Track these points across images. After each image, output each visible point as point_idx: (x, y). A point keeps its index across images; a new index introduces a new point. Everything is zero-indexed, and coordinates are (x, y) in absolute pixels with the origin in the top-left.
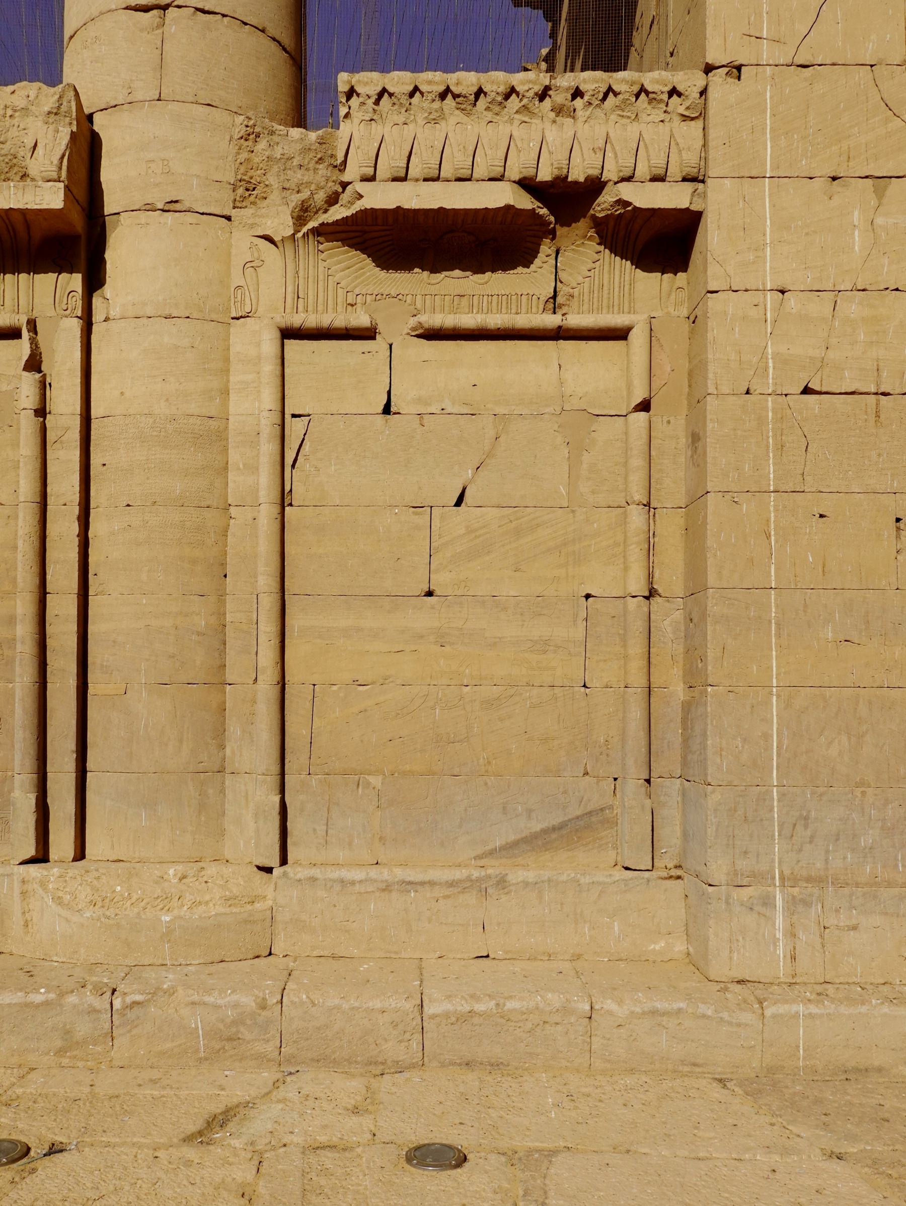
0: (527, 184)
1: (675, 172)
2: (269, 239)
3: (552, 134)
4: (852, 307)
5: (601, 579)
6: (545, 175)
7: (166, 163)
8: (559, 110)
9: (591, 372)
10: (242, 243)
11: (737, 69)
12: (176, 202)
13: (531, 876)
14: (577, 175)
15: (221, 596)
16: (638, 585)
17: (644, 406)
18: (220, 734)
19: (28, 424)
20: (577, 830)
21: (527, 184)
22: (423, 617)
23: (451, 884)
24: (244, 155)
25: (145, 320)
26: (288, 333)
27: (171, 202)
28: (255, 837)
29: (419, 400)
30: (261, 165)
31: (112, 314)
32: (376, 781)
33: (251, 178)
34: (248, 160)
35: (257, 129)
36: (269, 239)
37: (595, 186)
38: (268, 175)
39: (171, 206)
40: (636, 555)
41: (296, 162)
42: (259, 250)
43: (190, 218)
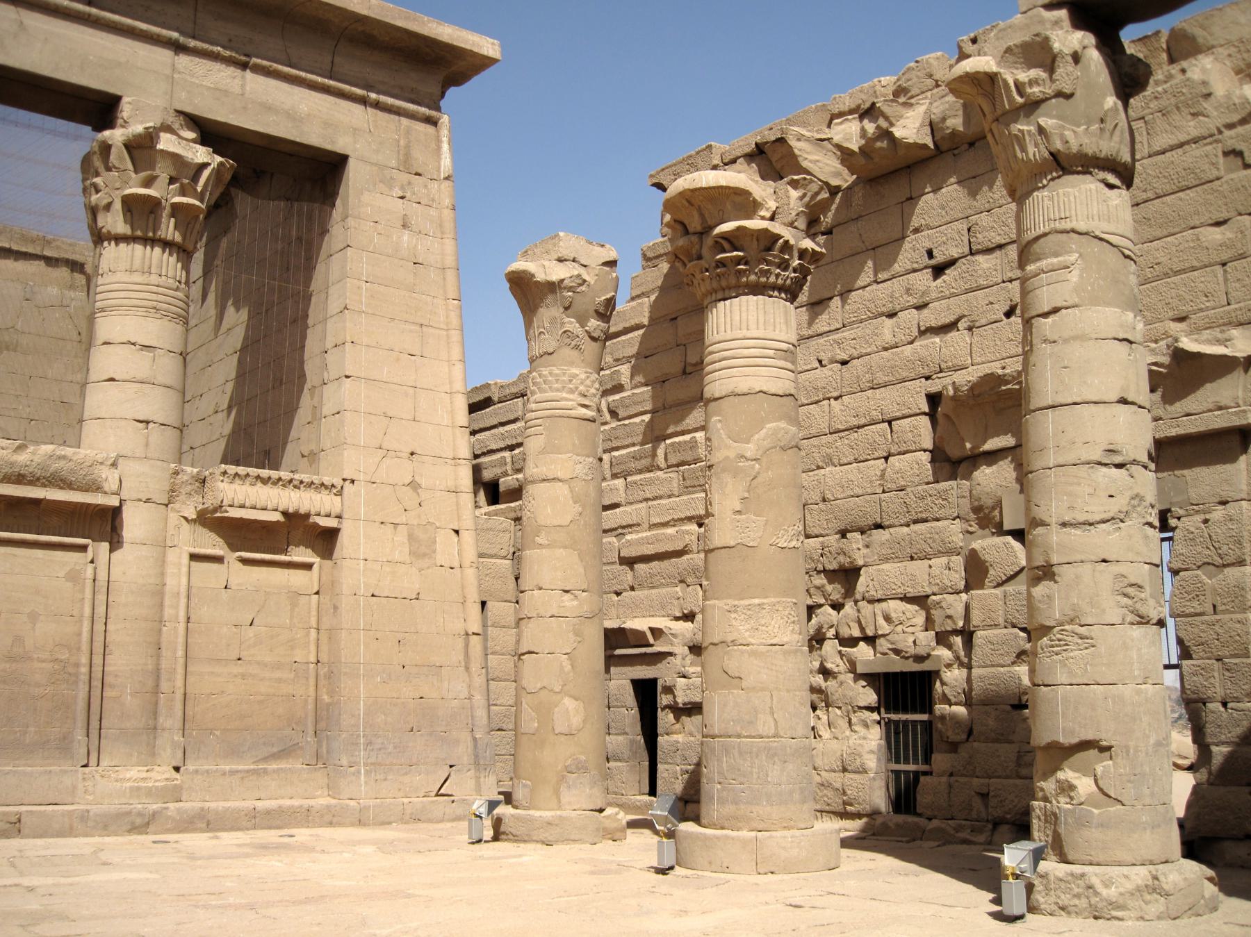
0: (285, 514)
1: (333, 514)
2: (185, 518)
3: (292, 494)
4: (387, 569)
5: (299, 655)
6: (291, 510)
8: (295, 487)
9: (297, 578)
10: (173, 518)
11: (353, 481)
13: (275, 766)
14: (302, 511)
15: (159, 657)
16: (313, 659)
17: (317, 593)
18: (155, 714)
19: (89, 583)
20: (284, 753)
21: (285, 514)
22: (237, 669)
23: (248, 771)
26: (194, 557)
28: (168, 755)
29: (239, 584)
32: (218, 733)
36: (185, 518)
37: (307, 515)
39: (148, 501)
40: (313, 648)
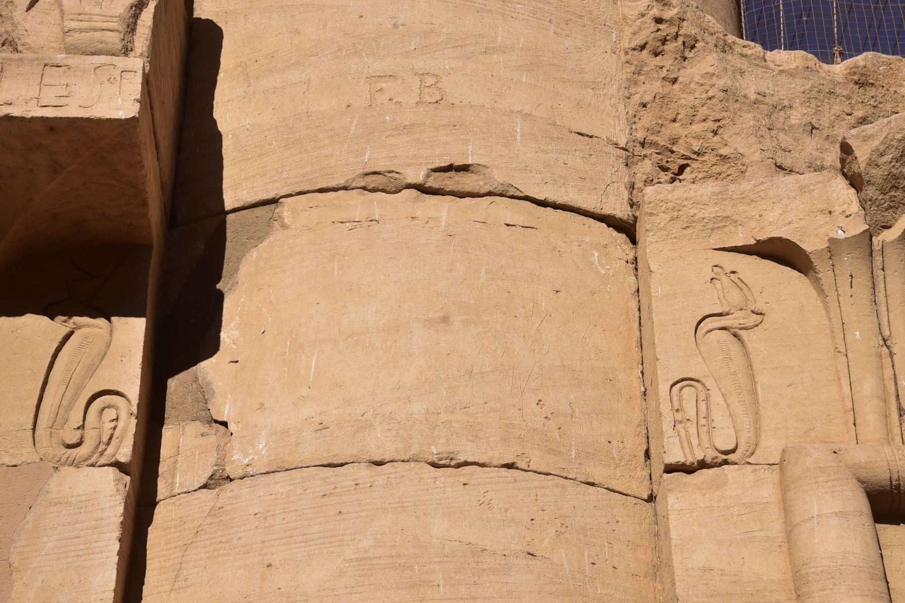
2: (781, 252)
7: (430, 81)
12: (465, 168)
24: (650, 88)
25: (364, 473)
27: (449, 168)
30: (704, 111)
31: (238, 460)
33: (674, 141)
34: (663, 99)
35: (688, 29)
36: (781, 252)
38: (726, 134)
39: (448, 181)
41: (796, 117)
42: (742, 285)
43: (504, 210)
